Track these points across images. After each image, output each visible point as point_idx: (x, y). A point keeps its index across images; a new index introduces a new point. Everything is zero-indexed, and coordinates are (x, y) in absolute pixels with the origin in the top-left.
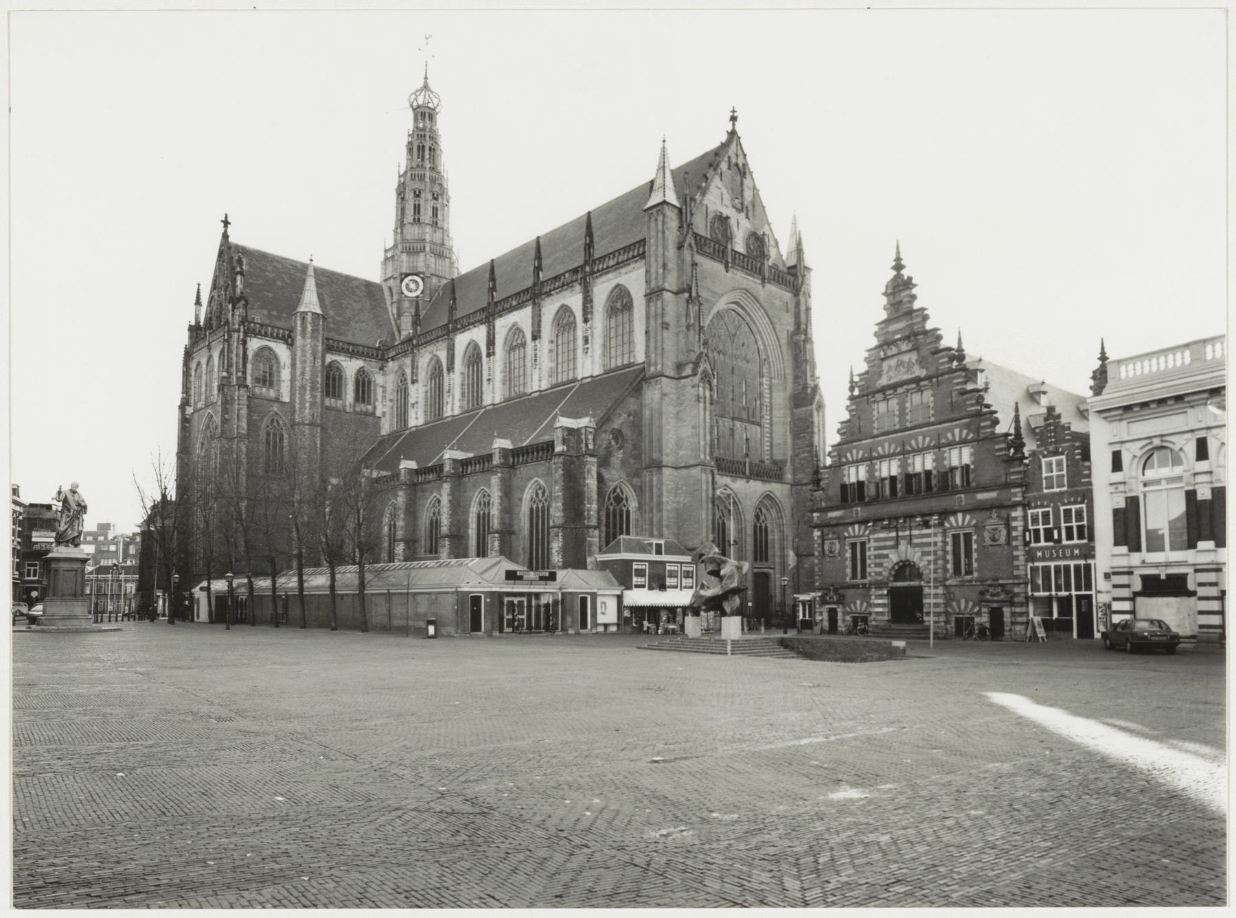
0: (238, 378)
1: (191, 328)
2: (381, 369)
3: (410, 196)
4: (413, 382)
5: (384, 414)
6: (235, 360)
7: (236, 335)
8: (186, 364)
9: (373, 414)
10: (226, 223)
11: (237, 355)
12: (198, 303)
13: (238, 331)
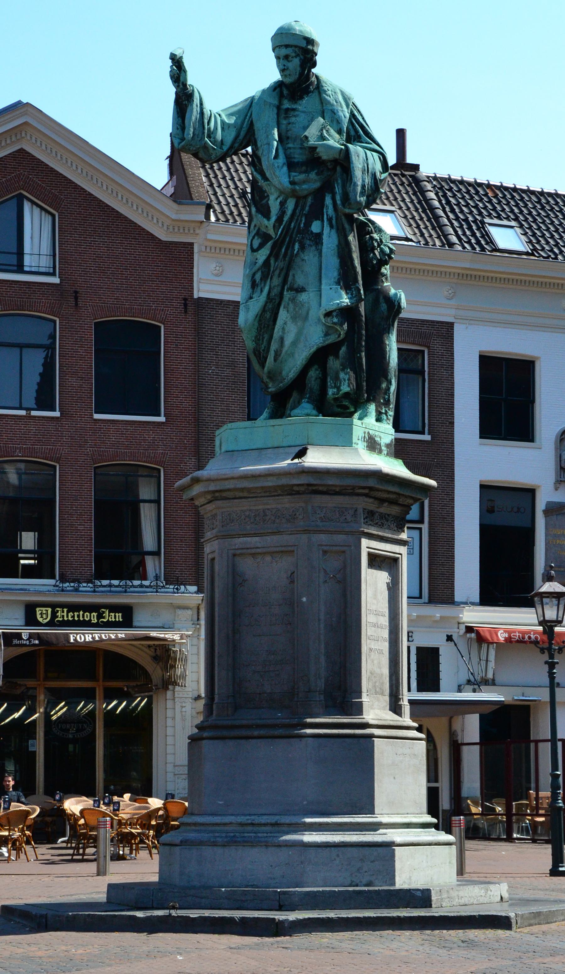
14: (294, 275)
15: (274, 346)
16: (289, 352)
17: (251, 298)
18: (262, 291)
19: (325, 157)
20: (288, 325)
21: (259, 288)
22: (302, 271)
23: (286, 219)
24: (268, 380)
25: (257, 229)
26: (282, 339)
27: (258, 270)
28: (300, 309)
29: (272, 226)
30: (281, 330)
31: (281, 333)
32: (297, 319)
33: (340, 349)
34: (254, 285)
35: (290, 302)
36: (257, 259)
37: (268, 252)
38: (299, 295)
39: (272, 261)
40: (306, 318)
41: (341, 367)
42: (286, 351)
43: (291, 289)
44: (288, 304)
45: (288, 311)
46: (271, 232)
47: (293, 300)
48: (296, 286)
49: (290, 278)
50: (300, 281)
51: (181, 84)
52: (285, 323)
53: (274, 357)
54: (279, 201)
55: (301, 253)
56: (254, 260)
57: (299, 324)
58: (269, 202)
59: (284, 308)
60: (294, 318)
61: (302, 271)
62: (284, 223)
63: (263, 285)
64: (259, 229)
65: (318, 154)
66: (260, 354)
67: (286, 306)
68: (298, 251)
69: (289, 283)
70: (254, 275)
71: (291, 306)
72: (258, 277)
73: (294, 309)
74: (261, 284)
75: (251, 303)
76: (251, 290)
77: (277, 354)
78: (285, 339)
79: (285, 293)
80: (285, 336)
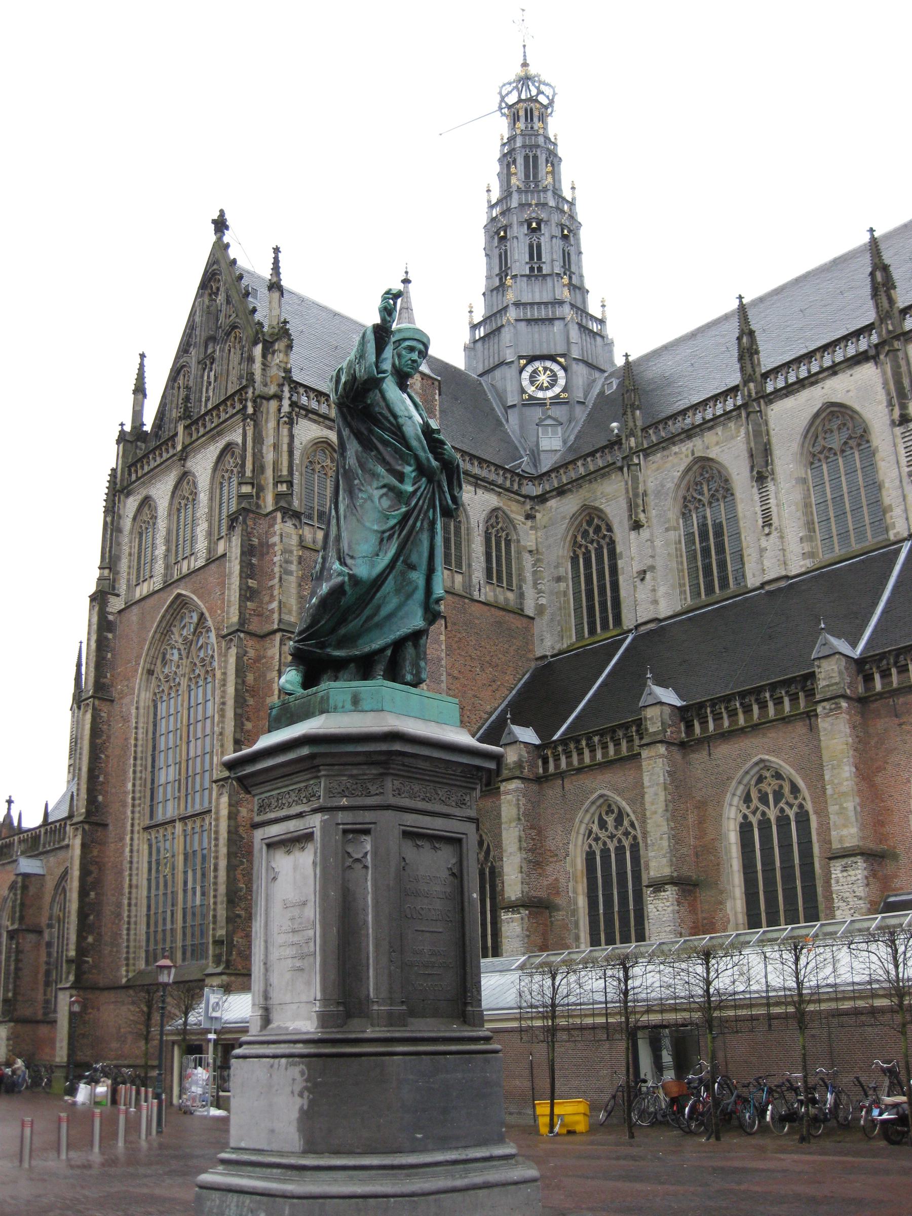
0: (278, 496)
1: (122, 438)
2: (529, 517)
3: (519, 232)
4: (637, 526)
5: (540, 609)
6: (269, 456)
7: (273, 404)
8: (112, 509)
9: (519, 612)
10: (220, 225)
11: (276, 447)
12: (140, 390)
13: (278, 397)
15: (367, 612)
17: (378, 555)
18: (386, 553)
19: (446, 457)
26: (378, 608)
28: (407, 585)
40: (409, 596)
47: (403, 574)
48: (409, 561)
50: (414, 558)
54: (414, 474)
60: (398, 591)
70: (383, 532)
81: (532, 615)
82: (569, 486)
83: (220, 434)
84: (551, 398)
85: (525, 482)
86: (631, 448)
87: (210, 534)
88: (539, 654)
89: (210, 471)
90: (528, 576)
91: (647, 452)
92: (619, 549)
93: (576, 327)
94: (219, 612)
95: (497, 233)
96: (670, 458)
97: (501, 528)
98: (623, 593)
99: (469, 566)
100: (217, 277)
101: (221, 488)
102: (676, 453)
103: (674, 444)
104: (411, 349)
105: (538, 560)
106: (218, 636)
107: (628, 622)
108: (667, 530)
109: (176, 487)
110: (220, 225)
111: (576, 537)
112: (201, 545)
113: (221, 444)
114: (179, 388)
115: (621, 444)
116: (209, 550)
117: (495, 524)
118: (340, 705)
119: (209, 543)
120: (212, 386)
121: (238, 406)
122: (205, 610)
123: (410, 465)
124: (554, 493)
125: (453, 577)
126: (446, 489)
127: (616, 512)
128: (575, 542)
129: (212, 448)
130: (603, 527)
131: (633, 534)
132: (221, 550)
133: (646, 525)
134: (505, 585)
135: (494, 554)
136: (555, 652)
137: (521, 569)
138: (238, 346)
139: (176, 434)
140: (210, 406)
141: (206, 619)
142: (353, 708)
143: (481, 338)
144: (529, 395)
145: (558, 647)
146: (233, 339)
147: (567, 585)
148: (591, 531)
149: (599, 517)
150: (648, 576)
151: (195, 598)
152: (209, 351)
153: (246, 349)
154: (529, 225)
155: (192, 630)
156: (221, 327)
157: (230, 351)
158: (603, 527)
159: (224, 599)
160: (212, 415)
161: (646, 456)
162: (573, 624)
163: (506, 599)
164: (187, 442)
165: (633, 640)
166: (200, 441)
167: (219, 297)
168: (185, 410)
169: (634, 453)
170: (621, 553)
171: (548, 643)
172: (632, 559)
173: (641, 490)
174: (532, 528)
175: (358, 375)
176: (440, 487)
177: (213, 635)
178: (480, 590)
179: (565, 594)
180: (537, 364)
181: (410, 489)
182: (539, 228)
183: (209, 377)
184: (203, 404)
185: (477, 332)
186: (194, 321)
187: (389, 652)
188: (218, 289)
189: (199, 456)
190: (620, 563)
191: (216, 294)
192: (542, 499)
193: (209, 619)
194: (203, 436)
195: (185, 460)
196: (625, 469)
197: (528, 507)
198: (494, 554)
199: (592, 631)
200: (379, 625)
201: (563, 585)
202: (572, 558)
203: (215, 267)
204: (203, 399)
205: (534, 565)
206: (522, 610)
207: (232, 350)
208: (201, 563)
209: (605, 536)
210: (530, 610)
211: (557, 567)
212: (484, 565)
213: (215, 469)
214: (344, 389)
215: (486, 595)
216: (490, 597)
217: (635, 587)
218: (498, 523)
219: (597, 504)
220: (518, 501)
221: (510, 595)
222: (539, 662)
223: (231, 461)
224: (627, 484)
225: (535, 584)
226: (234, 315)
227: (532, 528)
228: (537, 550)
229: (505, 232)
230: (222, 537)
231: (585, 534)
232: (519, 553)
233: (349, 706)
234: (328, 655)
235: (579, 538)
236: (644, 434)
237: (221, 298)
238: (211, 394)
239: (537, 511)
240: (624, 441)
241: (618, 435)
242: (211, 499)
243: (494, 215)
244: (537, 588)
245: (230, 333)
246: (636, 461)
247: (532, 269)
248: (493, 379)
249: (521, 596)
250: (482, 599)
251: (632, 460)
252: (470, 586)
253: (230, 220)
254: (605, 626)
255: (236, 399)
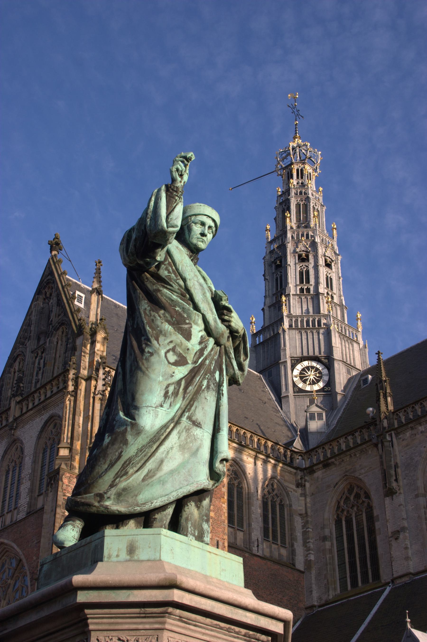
4: (390, 493)
9: (292, 565)
10: (55, 245)
14: (196, 407)
15: (150, 465)
16: (162, 479)
17: (162, 406)
20: (173, 451)
21: (169, 401)
22: (203, 408)
23: (206, 353)
24: (112, 497)
25: (171, 346)
26: (162, 462)
27: (173, 383)
28: (191, 442)
29: (195, 351)
30: (165, 453)
31: (164, 455)
32: (186, 451)
33: (205, 500)
34: (166, 395)
35: (185, 431)
36: (174, 373)
37: (186, 373)
38: (194, 427)
39: (183, 383)
41: (205, 518)
42: (161, 476)
43: (189, 418)
44: (182, 432)
45: (179, 438)
46: (190, 358)
47: (188, 430)
48: (194, 418)
49: (193, 408)
50: (199, 416)
51: (183, 182)
52: (172, 448)
53: (145, 476)
55: (206, 392)
56: (171, 372)
57: (186, 455)
58: (192, 330)
59: (178, 433)
60: (182, 448)
61: (203, 408)
62: (204, 356)
63: (172, 400)
64: (175, 346)
65: (231, 317)
66: (126, 467)
67: (180, 432)
68: (205, 388)
69: (191, 412)
71: (184, 434)
72: (171, 389)
73: (186, 439)
74: (171, 398)
75: (160, 409)
76: (163, 399)
77: (150, 475)
78: (164, 463)
79: (184, 419)
80: (166, 460)
81: (302, 569)
82: (333, 460)
83: (44, 408)
84: (317, 391)
85: (296, 456)
86: (384, 428)
87: (31, 491)
88: (308, 604)
89: (35, 439)
90: (299, 535)
91: (398, 431)
92: (376, 512)
93: (337, 335)
94: (35, 558)
95: (274, 262)
96: (418, 436)
97: (276, 494)
98: (380, 550)
99: (250, 525)
100: (50, 285)
101: (44, 453)
102: (422, 432)
103: (420, 424)
104: (203, 224)
105: (307, 522)
106: (32, 579)
107: (385, 577)
108: (417, 496)
109: (5, 452)
110: (55, 245)
111: (339, 503)
112: (24, 500)
113: (45, 417)
114: (15, 372)
115: (376, 425)
116: (30, 505)
117: (271, 491)
118: (115, 554)
119: (31, 499)
120: (42, 371)
121: (61, 386)
122: (22, 557)
123: (196, 324)
124: (321, 466)
125: (235, 534)
126: (233, 355)
127: (372, 481)
128: (338, 507)
129: (38, 420)
130: (362, 493)
131: (387, 500)
132: (39, 505)
133: (398, 492)
134: (279, 543)
135: (270, 516)
136: (323, 602)
137: (292, 530)
138: (64, 339)
139: (10, 408)
140: (38, 386)
141: (23, 566)
142: (128, 557)
143: (260, 343)
144: (299, 388)
145: (325, 598)
146: (60, 333)
147: (332, 544)
148: (352, 498)
149: (358, 487)
150: (401, 536)
151: (15, 547)
152: (41, 342)
153: (70, 341)
154: (300, 256)
155: (10, 574)
156: (51, 324)
157: (57, 343)
158: (362, 493)
159: (39, 547)
160: (40, 393)
161: (397, 434)
162: (338, 578)
163: (280, 555)
164: (17, 414)
165: (390, 592)
166: (29, 414)
167: (51, 301)
168: (17, 389)
169: (387, 432)
170: (378, 516)
171: (315, 594)
172: (387, 521)
173: (393, 463)
174: (301, 495)
175: (148, 229)
176: (227, 353)
177: (28, 579)
178: (258, 546)
179: (331, 551)
180: (306, 363)
181: (198, 347)
182: (307, 256)
183: (39, 364)
184: (33, 385)
185: (257, 339)
186: (30, 319)
187: (170, 511)
188: (51, 295)
189: (27, 427)
190: (378, 525)
191: (50, 298)
192: (310, 470)
193: (26, 564)
194: (31, 409)
195: (15, 429)
196: (380, 446)
197: (299, 477)
198: (270, 516)
199: (354, 584)
200: (162, 482)
201: (328, 544)
202: (336, 521)
203: (49, 277)
204: (34, 382)
205: (303, 527)
206: (294, 565)
207: (60, 342)
208: (22, 515)
209: (363, 502)
210: (300, 565)
211: (323, 528)
212: (261, 524)
213: (39, 437)
214: (135, 246)
215: (263, 551)
216: (267, 553)
217: (390, 545)
218: (273, 490)
219: (357, 474)
220: (290, 473)
221: (284, 552)
222: (308, 611)
223: (53, 431)
224: (381, 457)
225: (305, 543)
226: (62, 315)
227: (301, 495)
228: (306, 513)
229: (281, 262)
230: (42, 494)
231: (347, 498)
232: (291, 515)
233: (124, 556)
234: (106, 508)
235: (342, 503)
236: (395, 417)
237: (53, 301)
238: (40, 377)
239: (305, 481)
240: (378, 423)
241: (373, 418)
242: (34, 462)
243: (272, 249)
244: (306, 547)
245: (58, 329)
246: (388, 438)
247: (302, 290)
248: (270, 375)
249: (293, 552)
250: (260, 553)
251: (385, 438)
252: (250, 542)
253: (64, 242)
254: (365, 580)
255: (60, 380)
